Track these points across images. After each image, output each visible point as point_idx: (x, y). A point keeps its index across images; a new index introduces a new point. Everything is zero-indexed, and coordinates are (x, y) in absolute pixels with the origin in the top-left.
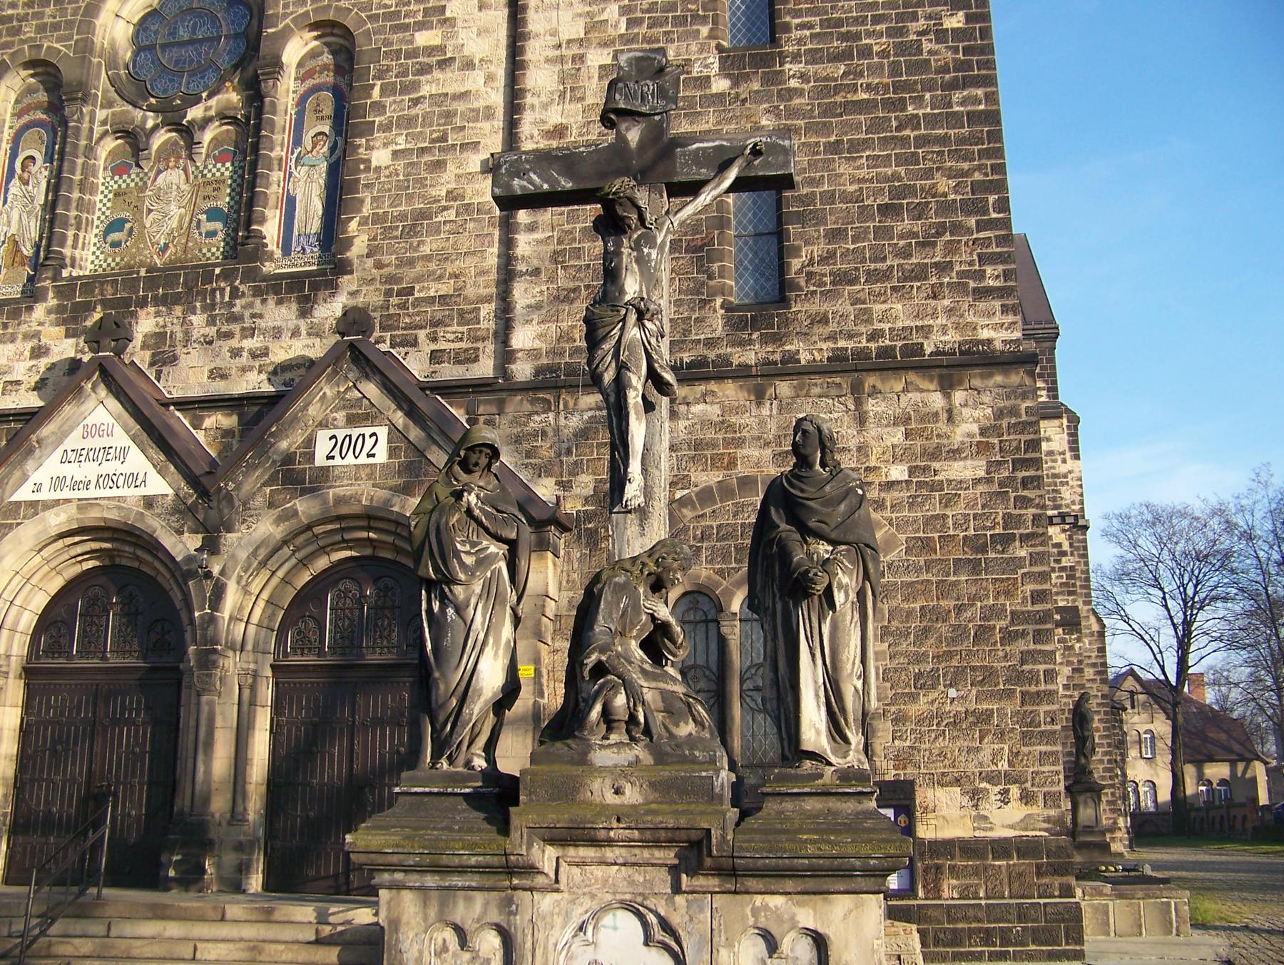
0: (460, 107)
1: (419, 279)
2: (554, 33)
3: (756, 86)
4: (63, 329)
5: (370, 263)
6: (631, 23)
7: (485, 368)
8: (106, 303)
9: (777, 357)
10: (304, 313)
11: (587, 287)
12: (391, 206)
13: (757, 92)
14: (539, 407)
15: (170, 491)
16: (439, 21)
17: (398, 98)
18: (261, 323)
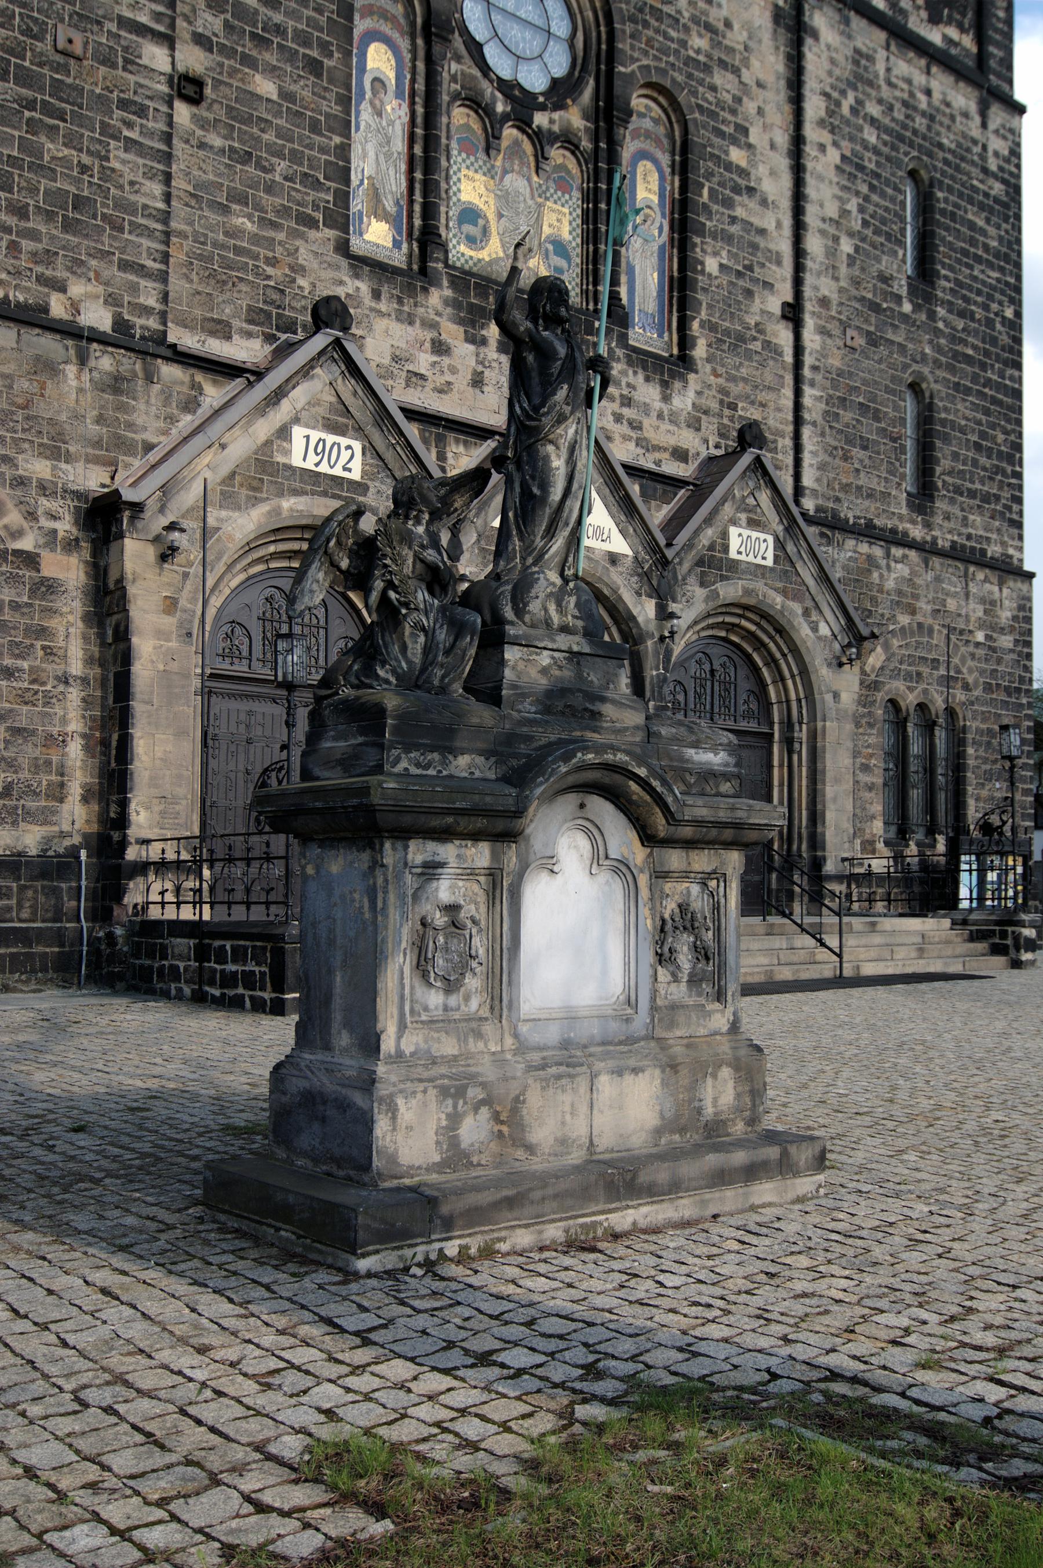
5: (708, 368)
6: (865, 223)
10: (666, 398)
15: (630, 553)
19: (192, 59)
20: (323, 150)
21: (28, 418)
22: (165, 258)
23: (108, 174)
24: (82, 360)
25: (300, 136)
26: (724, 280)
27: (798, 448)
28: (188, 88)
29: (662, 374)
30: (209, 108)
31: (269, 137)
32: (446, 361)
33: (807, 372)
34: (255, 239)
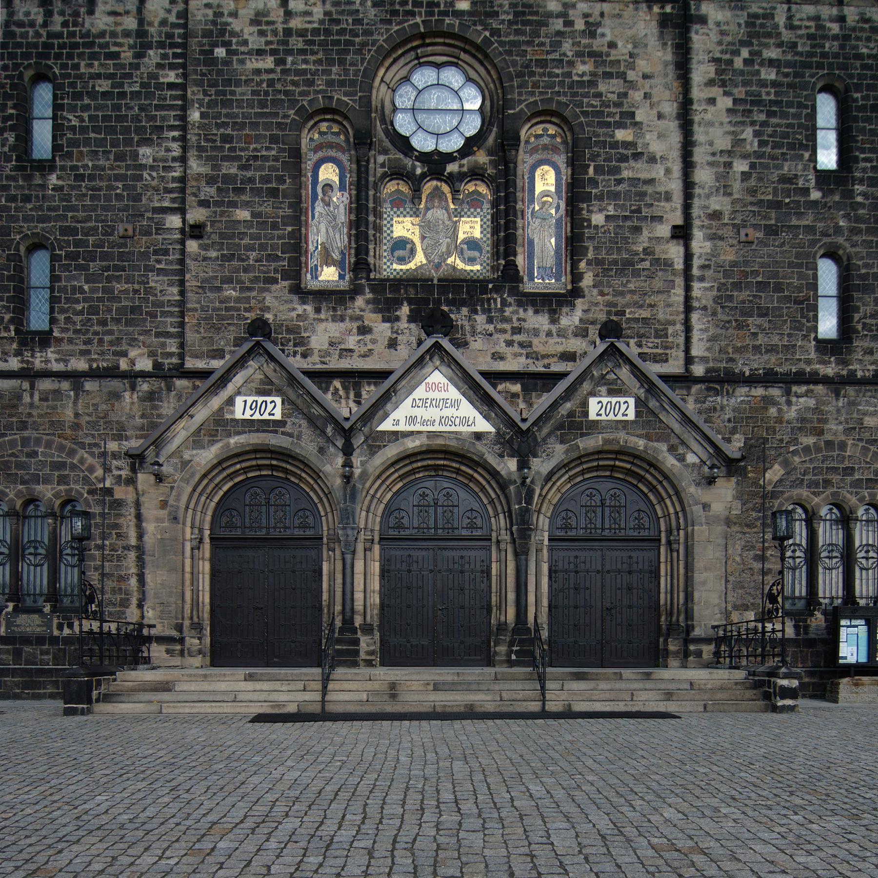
0: (649, 189)
1: (628, 305)
2: (711, 144)
3: (837, 198)
4: (380, 315)
6: (762, 143)
7: (675, 366)
8: (410, 302)
9: (844, 372)
10: (554, 321)
11: (736, 321)
12: (607, 254)
13: (838, 202)
14: (711, 393)
16: (631, 124)
17: (607, 177)
18: (526, 325)
19: (196, 215)
20: (279, 238)
21: (105, 423)
22: (182, 325)
23: (149, 291)
24: (133, 388)
25: (265, 236)
26: (611, 226)
27: (688, 329)
28: (196, 231)
29: (551, 305)
30: (209, 238)
31: (246, 241)
32: (368, 337)
33: (695, 271)
34: (238, 300)
